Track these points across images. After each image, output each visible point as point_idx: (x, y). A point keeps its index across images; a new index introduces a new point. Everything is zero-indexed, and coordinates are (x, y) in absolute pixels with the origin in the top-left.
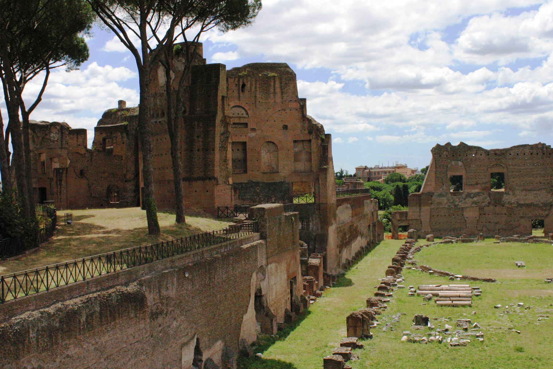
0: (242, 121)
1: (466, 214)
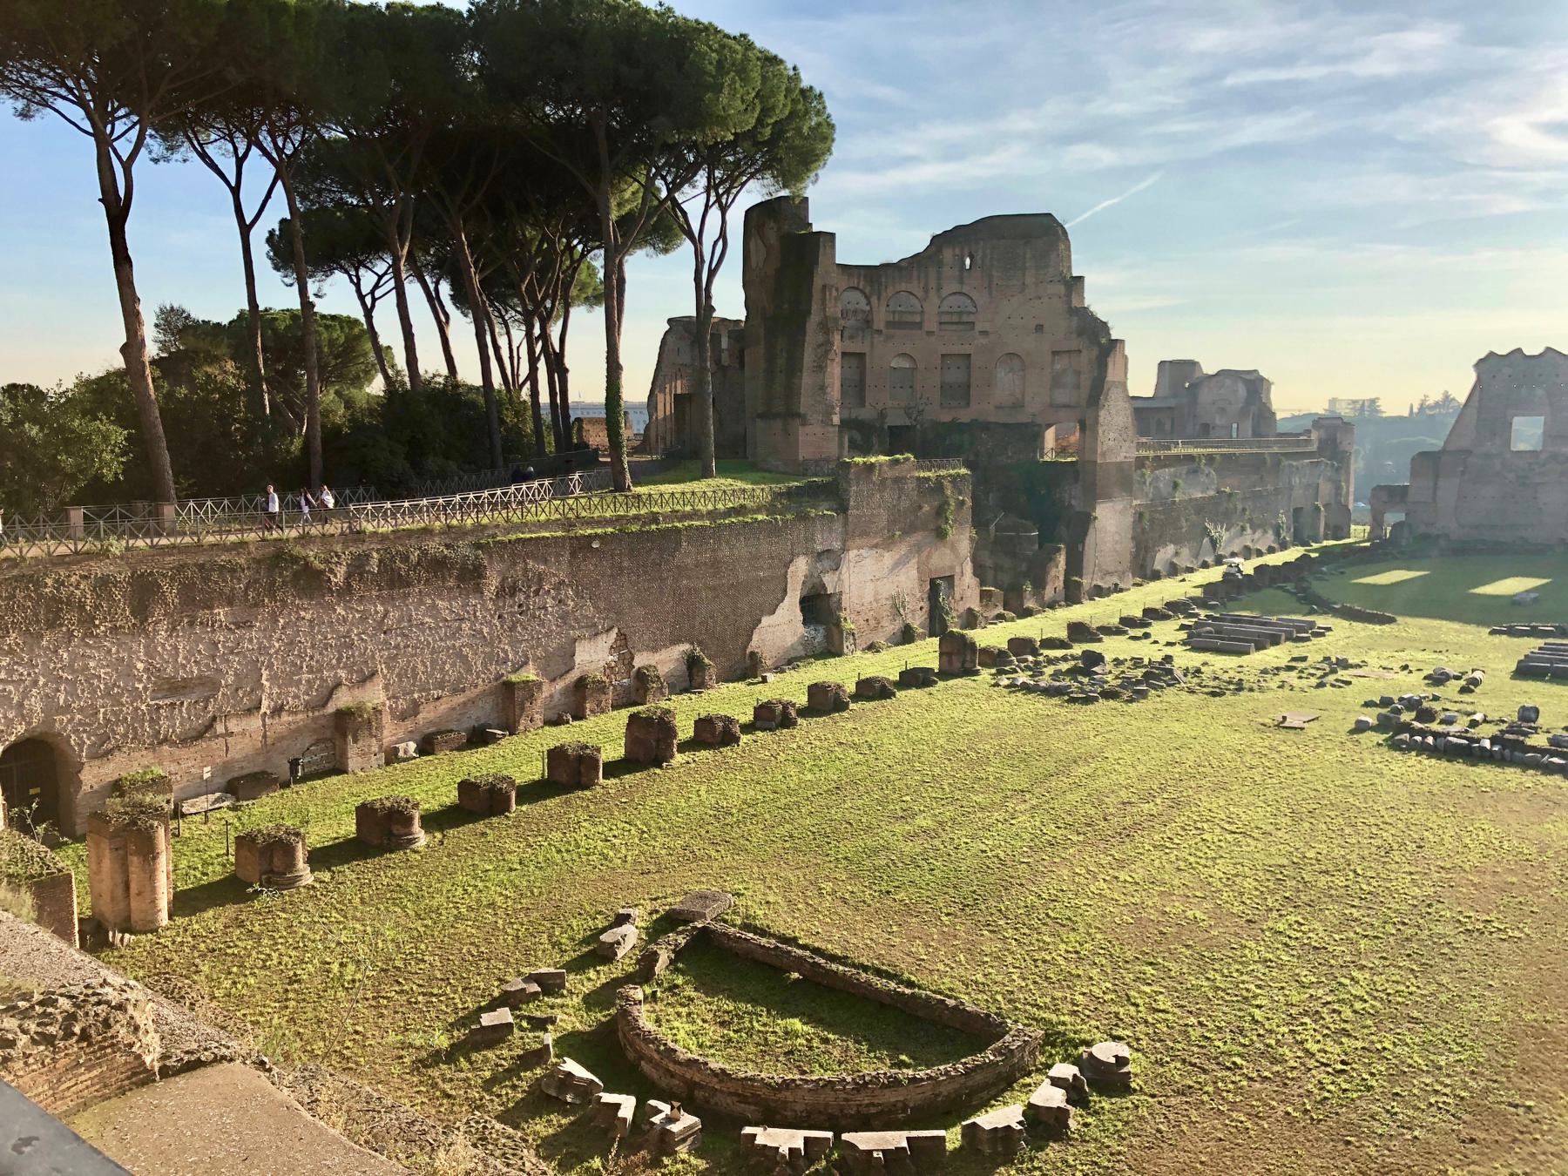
0: (965, 318)
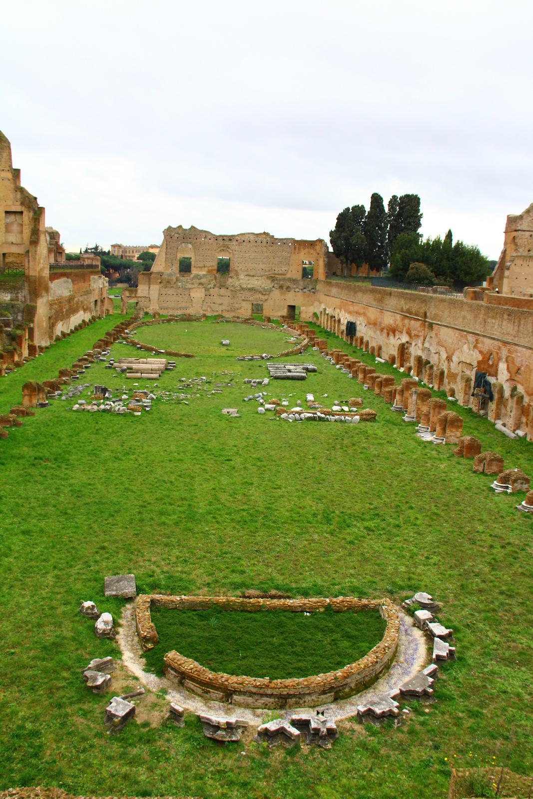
1: (192, 295)
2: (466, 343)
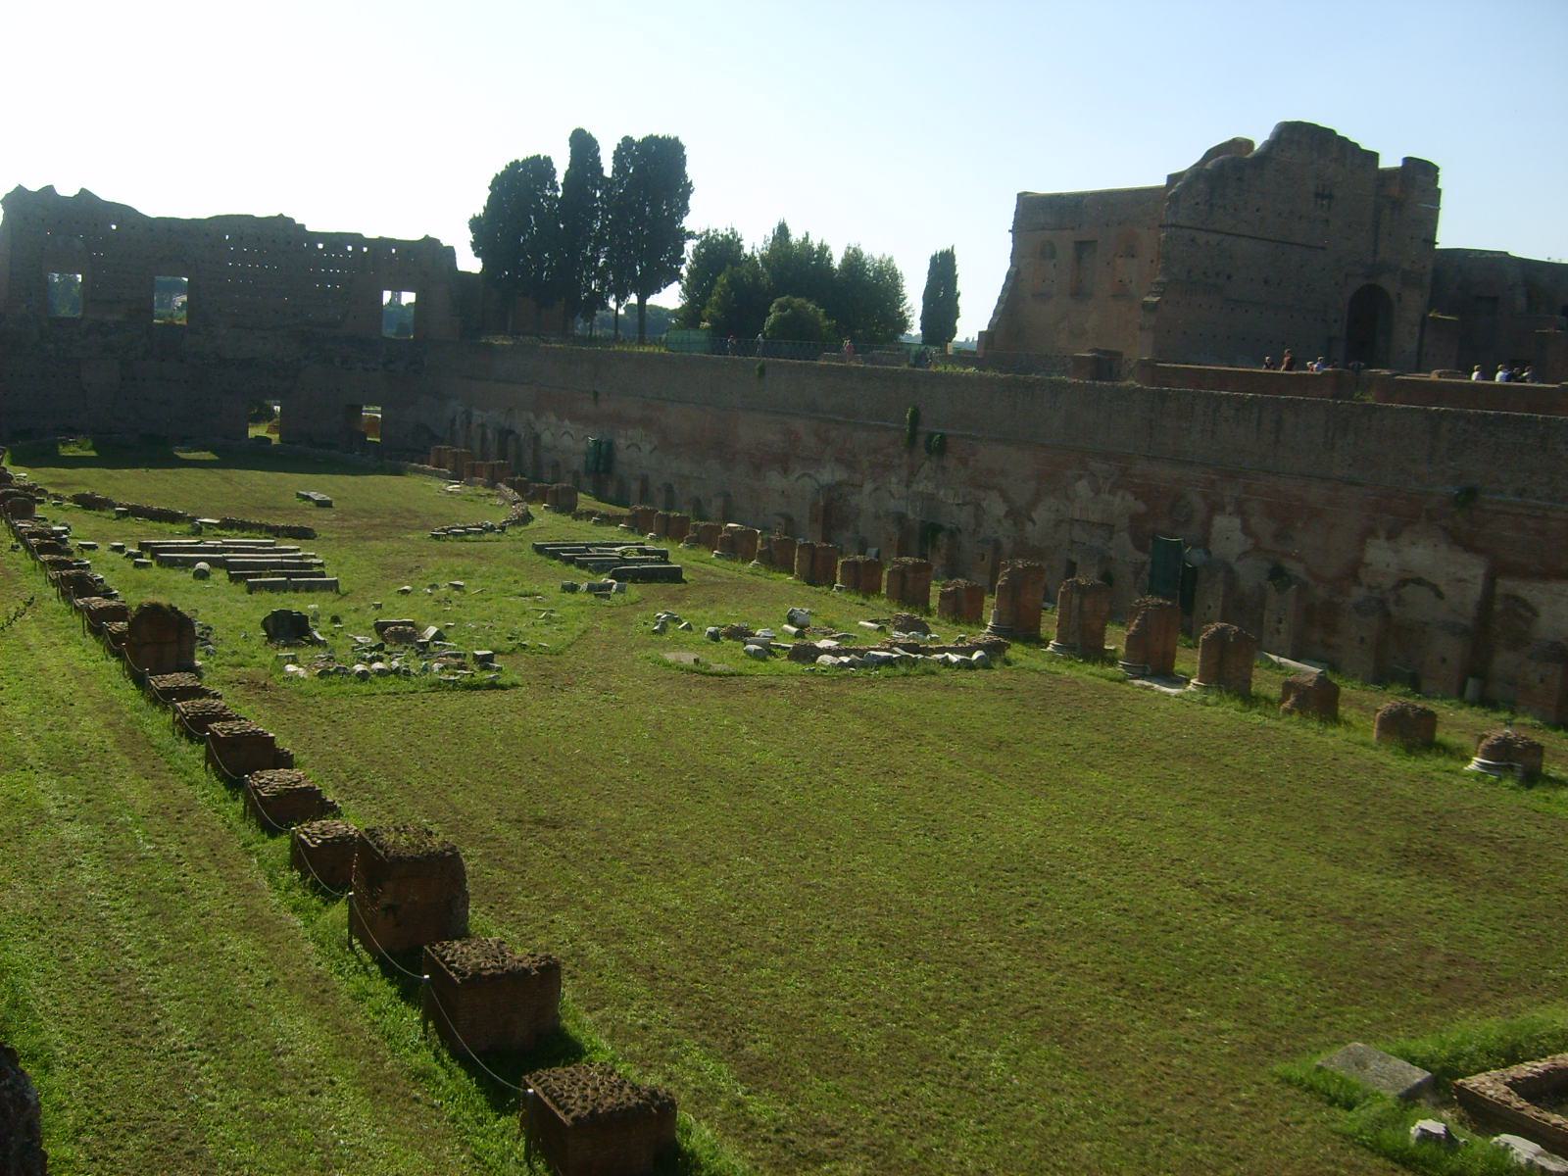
2: (1080, 477)
